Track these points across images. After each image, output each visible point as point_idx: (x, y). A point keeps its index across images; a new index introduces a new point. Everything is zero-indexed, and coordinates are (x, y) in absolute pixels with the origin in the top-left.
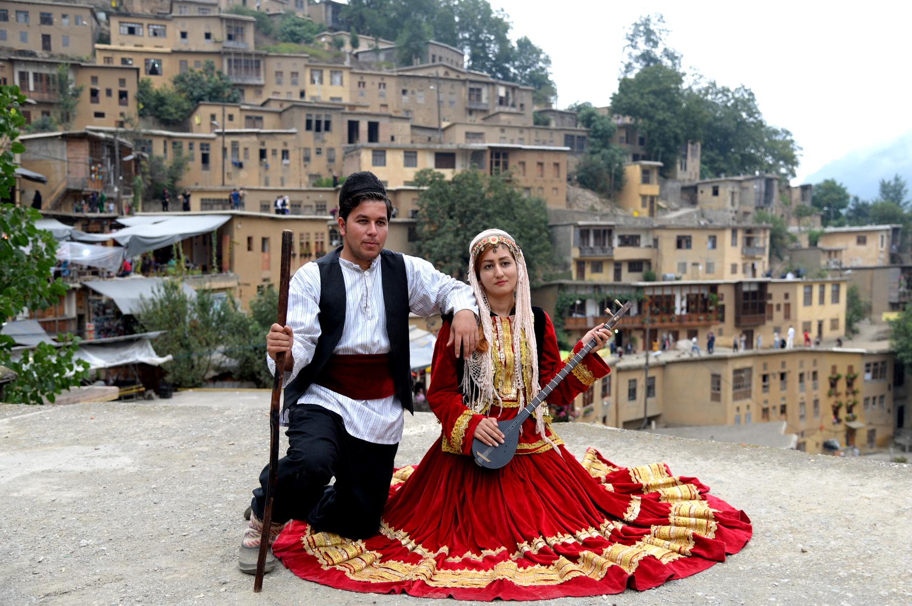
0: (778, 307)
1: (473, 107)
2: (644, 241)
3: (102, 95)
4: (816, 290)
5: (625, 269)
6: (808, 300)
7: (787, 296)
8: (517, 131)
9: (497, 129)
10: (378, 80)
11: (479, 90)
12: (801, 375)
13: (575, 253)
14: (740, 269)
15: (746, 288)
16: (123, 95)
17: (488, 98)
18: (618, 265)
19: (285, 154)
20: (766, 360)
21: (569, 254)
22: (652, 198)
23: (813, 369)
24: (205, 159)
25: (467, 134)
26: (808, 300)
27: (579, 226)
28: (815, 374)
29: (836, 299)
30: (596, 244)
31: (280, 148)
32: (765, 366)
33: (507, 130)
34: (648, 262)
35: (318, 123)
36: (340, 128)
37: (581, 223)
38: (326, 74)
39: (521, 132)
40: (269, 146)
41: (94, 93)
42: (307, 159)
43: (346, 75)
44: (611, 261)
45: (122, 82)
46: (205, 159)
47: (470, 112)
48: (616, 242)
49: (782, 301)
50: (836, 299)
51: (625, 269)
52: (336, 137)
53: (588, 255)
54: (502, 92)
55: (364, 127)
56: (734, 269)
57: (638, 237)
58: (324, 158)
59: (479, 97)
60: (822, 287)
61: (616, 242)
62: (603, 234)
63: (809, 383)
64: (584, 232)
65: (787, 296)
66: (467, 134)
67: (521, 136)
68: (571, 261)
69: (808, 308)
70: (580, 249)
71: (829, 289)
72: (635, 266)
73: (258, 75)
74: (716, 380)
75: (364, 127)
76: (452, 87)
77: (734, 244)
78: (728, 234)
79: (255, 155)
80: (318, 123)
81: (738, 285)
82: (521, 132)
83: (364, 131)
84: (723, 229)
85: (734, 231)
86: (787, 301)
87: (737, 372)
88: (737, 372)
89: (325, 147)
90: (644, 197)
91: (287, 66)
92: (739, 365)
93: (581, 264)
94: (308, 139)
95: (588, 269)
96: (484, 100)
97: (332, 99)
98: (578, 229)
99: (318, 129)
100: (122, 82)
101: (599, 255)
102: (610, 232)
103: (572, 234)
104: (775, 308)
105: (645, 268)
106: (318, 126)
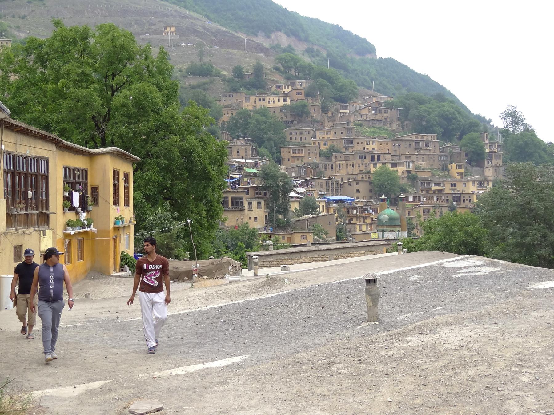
3: (311, 153)
7: (470, 197)
10: (386, 143)
15: (454, 195)
16: (316, 153)
18: (434, 191)
19: (353, 166)
22: (462, 173)
24: (332, 168)
31: (352, 164)
35: (362, 157)
36: (368, 158)
38: (371, 143)
40: (349, 164)
41: (309, 152)
42: (359, 166)
43: (376, 142)
45: (315, 150)
46: (332, 168)
48: (433, 185)
52: (368, 160)
55: (376, 157)
58: (364, 165)
59: (419, 145)
62: (429, 183)
65: (470, 197)
73: (352, 143)
75: (376, 157)
77: (474, 184)
78: (471, 183)
79: (345, 166)
80: (362, 157)
83: (375, 158)
84: (468, 181)
85: (474, 182)
89: (364, 163)
91: (360, 141)
94: (360, 161)
97: (373, 149)
99: (362, 158)
100: (315, 150)
101: (427, 189)
103: (420, 182)
106: (362, 157)
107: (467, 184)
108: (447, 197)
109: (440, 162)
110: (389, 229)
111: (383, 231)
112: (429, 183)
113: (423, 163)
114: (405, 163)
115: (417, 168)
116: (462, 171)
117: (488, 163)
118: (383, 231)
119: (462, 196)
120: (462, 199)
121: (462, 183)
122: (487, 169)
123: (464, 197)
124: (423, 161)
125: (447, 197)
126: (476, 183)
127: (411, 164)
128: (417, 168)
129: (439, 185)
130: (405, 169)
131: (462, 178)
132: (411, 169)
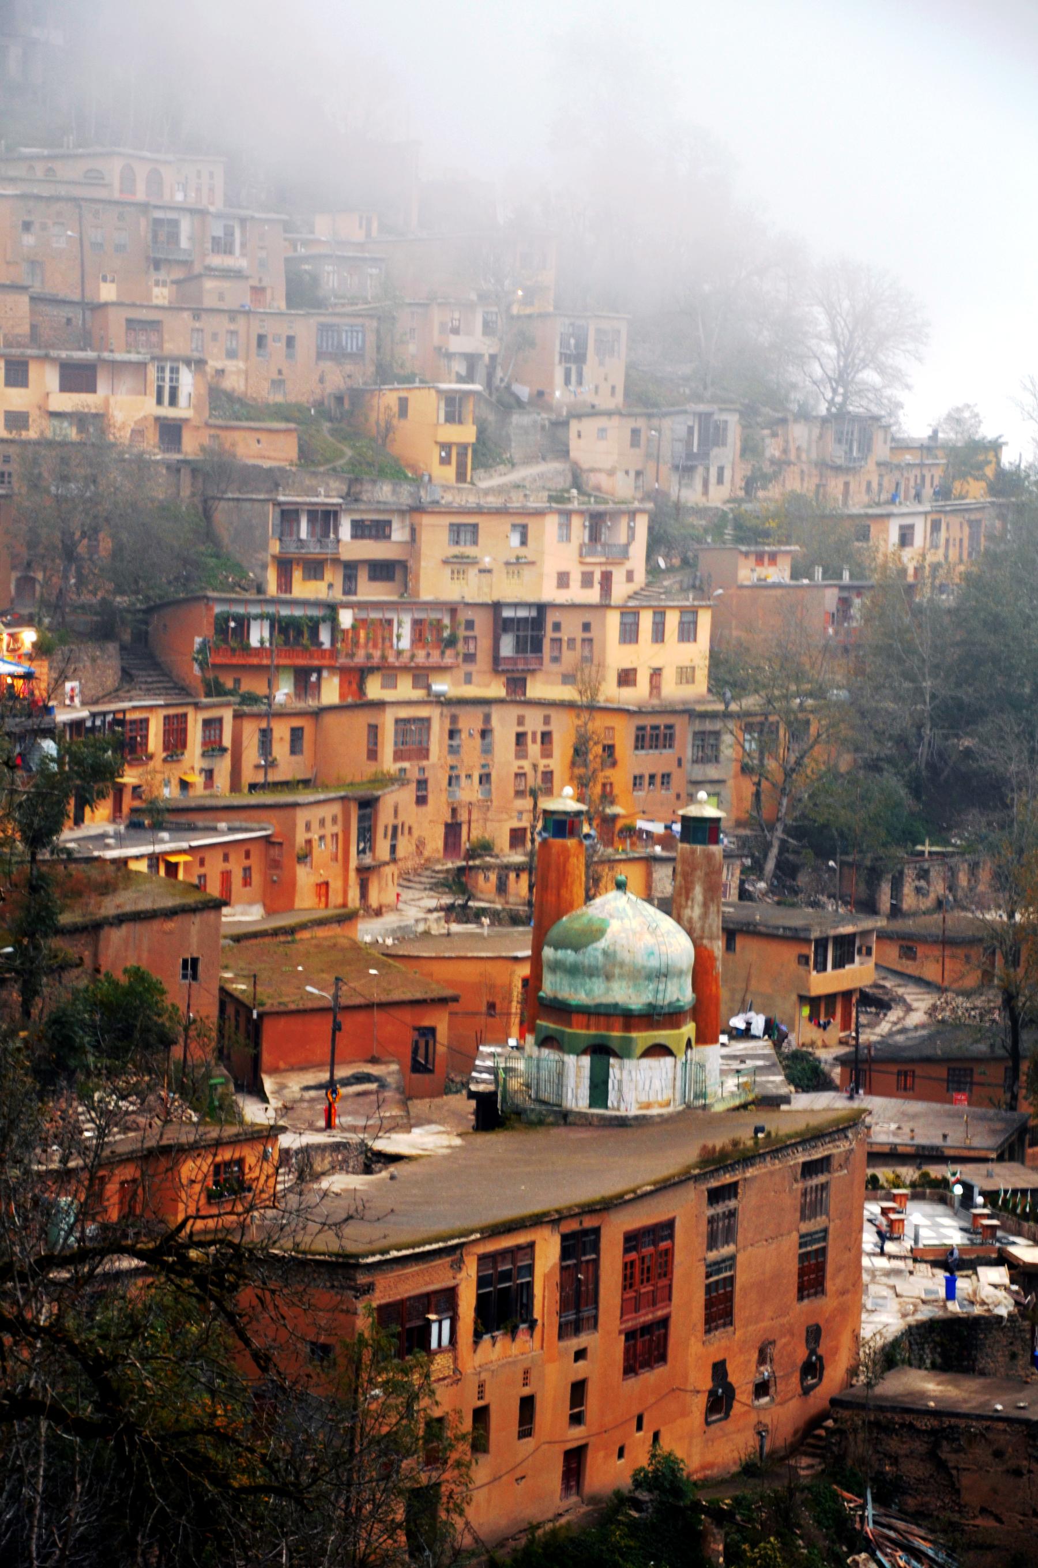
0: (572, 641)
1: (160, 256)
2: (399, 533)
4: (646, 620)
5: (363, 575)
6: (629, 634)
7: (586, 627)
8: (224, 319)
9: (186, 315)
11: (175, 223)
12: (520, 737)
13: (275, 548)
14: (575, 579)
15: (507, 613)
17: (190, 239)
18: (350, 570)
20: (455, 710)
21: (265, 547)
22: (463, 447)
23: (541, 728)
25: (129, 322)
26: (629, 634)
27: (279, 504)
28: (546, 737)
29: (687, 633)
30: (312, 533)
32: (454, 719)
33: (204, 316)
34: (403, 565)
37: (282, 498)
39: (232, 320)
44: (336, 561)
47: (157, 264)
48: (345, 531)
49: (579, 635)
50: (687, 633)
51: (363, 575)
53: (292, 549)
54: (217, 230)
56: (563, 581)
57: (389, 523)
59: (174, 237)
60: (660, 614)
61: (345, 531)
62: (325, 519)
63: (534, 749)
64: (289, 516)
65: (586, 627)
66: (129, 322)
67: (232, 327)
68: (269, 559)
69: (630, 648)
70: (280, 540)
71: (672, 620)
72: (383, 570)
74: (374, 730)
76: (121, 217)
78: (551, 524)
81: (497, 607)
82: (232, 320)
84: (539, 513)
86: (587, 635)
87: (397, 721)
88: (397, 721)
90: (446, 446)
92: (404, 713)
93: (285, 566)
95: (297, 574)
96: (184, 243)
98: (278, 510)
101: (314, 550)
102: (336, 513)
103: (272, 515)
104: (565, 646)
105: (398, 575)
107: (532, 524)
108: (470, 625)
109: (327, 365)
110: (643, 1038)
111: (601, 1052)
112: (325, 519)
113: (231, 365)
114: (152, 372)
115: (219, 400)
116: (467, 433)
117: (567, 381)
118: (601, 1052)
119: (551, 617)
120: (549, 633)
121: (504, 525)
122: (589, 426)
123: (557, 627)
124: (231, 354)
125: (470, 625)
126: (576, 522)
127: (187, 380)
128: (219, 400)
129: (378, 530)
130: (148, 407)
131: (461, 476)
132: (183, 411)
